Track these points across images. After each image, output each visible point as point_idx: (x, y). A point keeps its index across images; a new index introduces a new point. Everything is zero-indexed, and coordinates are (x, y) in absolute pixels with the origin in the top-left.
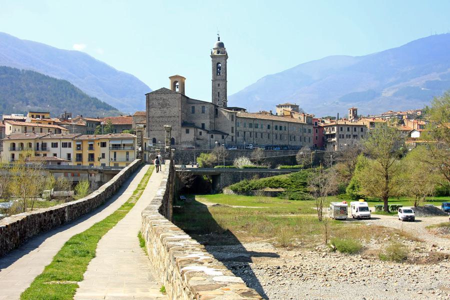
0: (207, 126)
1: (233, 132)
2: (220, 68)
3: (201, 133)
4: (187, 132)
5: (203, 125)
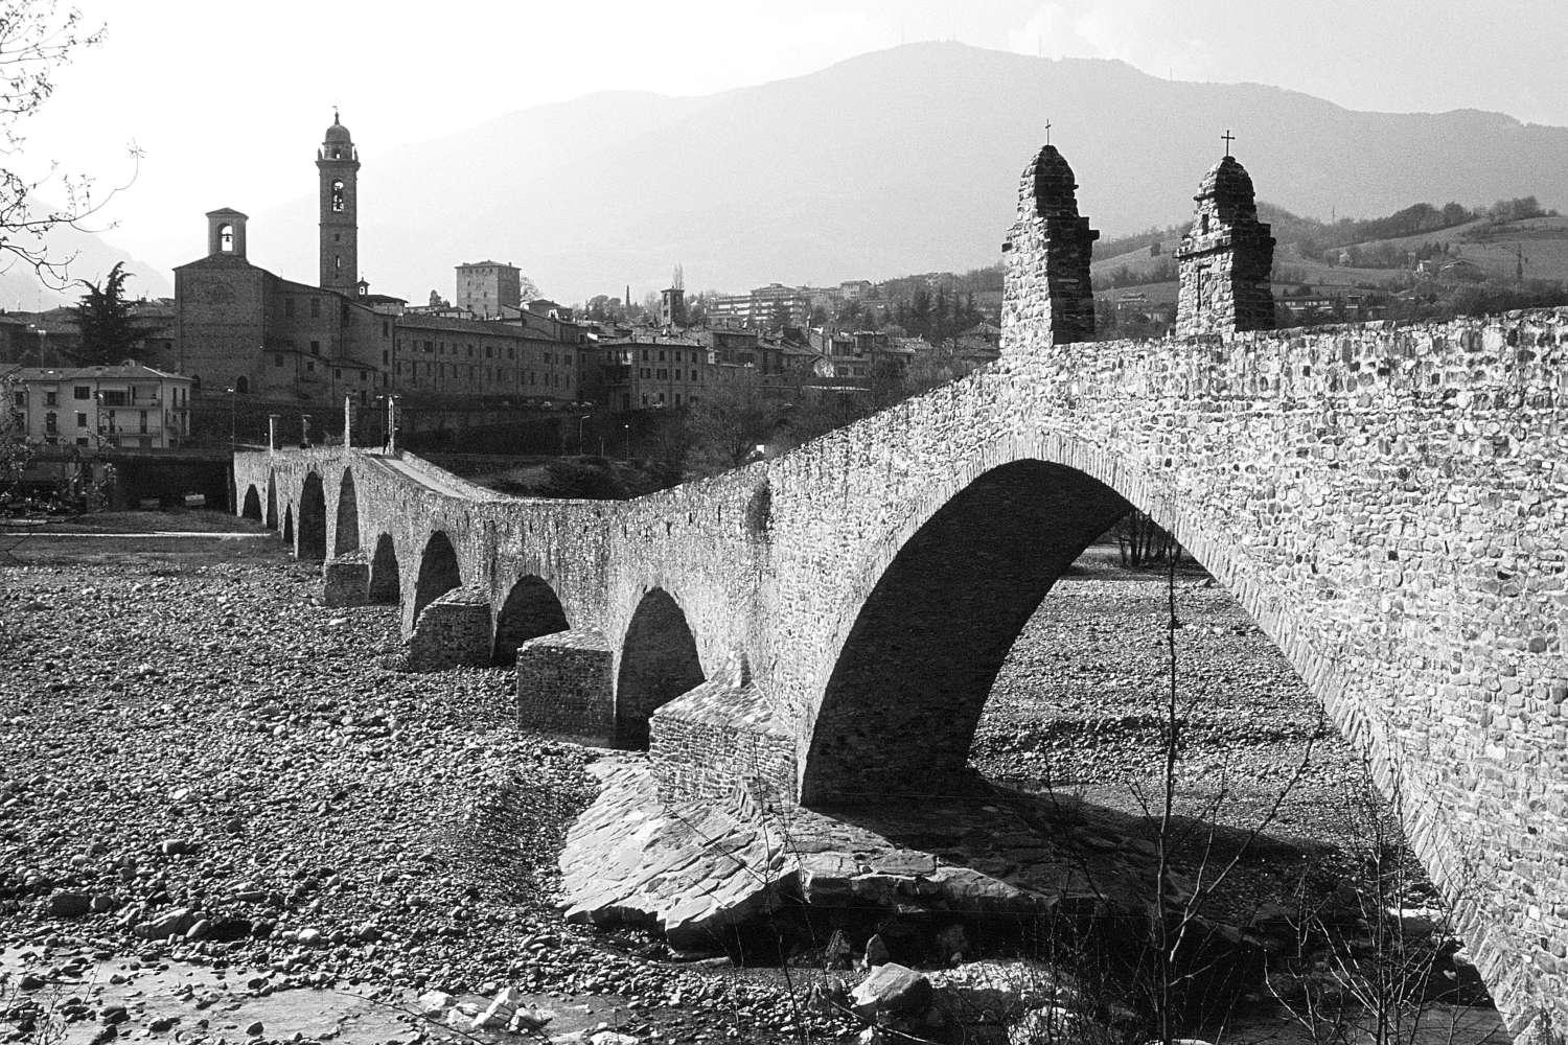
0: (325, 349)
1: (386, 361)
2: (340, 193)
3: (311, 366)
4: (279, 362)
5: (315, 345)
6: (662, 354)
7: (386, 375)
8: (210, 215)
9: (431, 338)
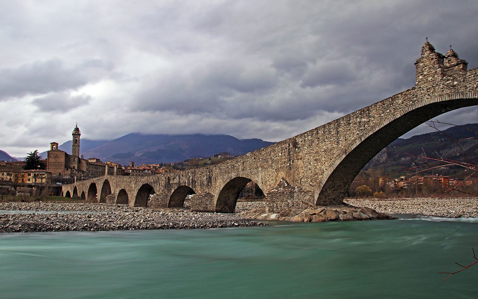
1: (87, 171)
3: (73, 171)
5: (74, 167)
6: (136, 171)
7: (87, 173)
8: (51, 143)
9: (95, 166)
